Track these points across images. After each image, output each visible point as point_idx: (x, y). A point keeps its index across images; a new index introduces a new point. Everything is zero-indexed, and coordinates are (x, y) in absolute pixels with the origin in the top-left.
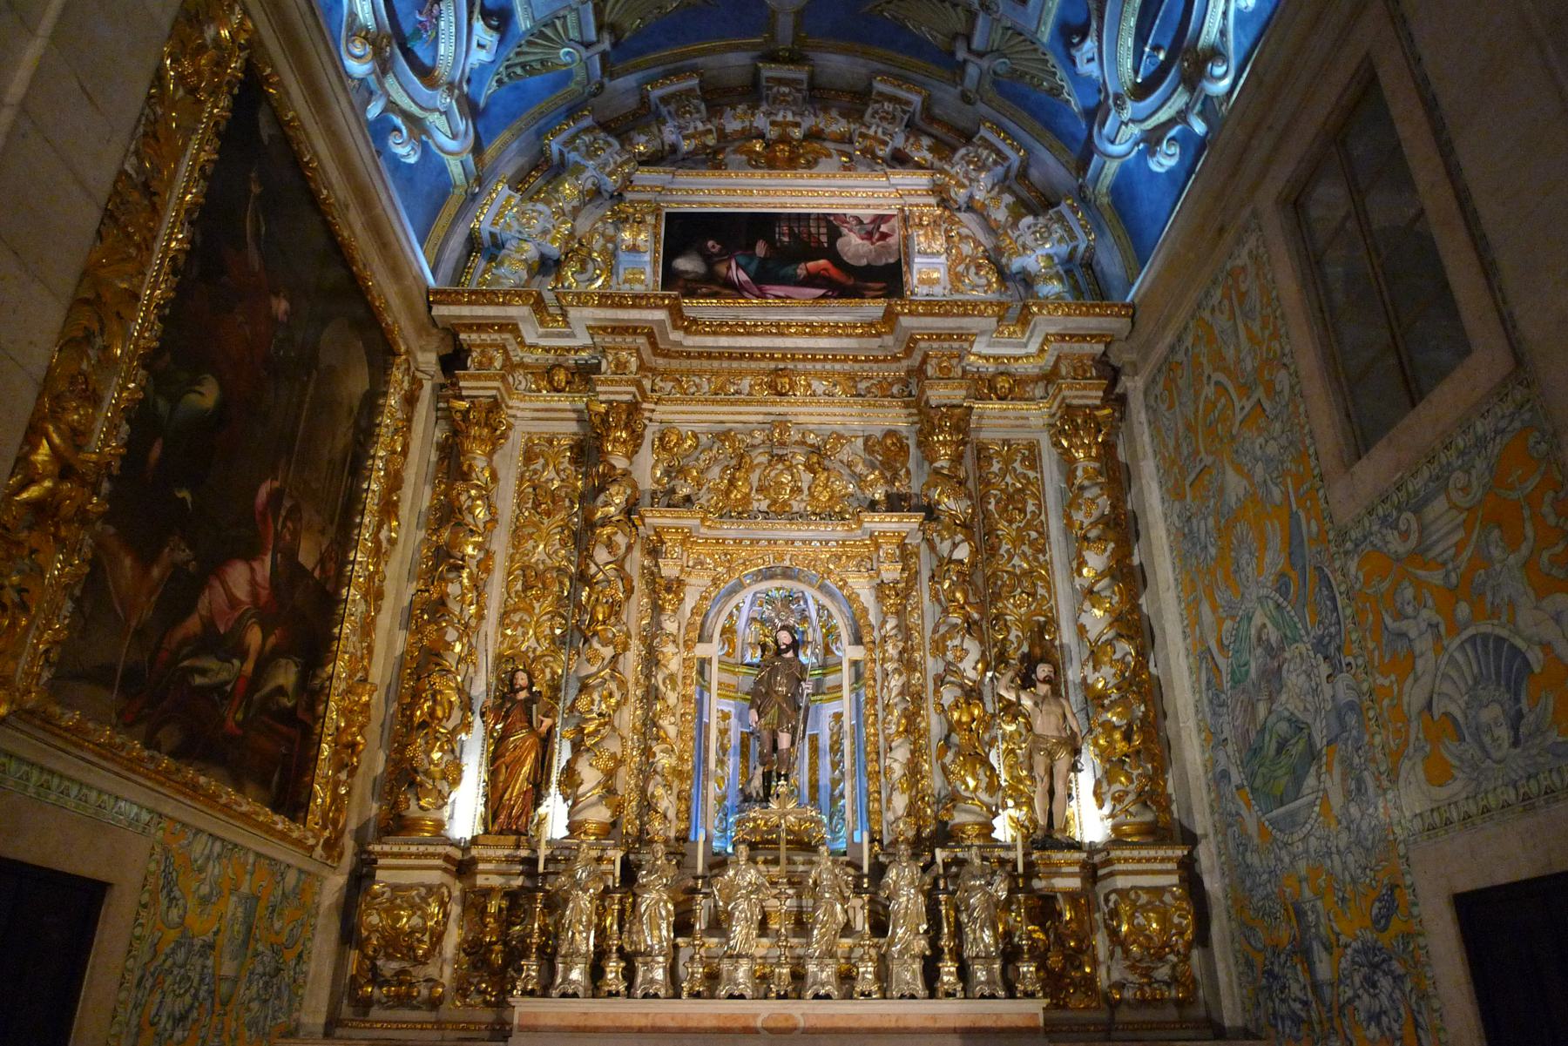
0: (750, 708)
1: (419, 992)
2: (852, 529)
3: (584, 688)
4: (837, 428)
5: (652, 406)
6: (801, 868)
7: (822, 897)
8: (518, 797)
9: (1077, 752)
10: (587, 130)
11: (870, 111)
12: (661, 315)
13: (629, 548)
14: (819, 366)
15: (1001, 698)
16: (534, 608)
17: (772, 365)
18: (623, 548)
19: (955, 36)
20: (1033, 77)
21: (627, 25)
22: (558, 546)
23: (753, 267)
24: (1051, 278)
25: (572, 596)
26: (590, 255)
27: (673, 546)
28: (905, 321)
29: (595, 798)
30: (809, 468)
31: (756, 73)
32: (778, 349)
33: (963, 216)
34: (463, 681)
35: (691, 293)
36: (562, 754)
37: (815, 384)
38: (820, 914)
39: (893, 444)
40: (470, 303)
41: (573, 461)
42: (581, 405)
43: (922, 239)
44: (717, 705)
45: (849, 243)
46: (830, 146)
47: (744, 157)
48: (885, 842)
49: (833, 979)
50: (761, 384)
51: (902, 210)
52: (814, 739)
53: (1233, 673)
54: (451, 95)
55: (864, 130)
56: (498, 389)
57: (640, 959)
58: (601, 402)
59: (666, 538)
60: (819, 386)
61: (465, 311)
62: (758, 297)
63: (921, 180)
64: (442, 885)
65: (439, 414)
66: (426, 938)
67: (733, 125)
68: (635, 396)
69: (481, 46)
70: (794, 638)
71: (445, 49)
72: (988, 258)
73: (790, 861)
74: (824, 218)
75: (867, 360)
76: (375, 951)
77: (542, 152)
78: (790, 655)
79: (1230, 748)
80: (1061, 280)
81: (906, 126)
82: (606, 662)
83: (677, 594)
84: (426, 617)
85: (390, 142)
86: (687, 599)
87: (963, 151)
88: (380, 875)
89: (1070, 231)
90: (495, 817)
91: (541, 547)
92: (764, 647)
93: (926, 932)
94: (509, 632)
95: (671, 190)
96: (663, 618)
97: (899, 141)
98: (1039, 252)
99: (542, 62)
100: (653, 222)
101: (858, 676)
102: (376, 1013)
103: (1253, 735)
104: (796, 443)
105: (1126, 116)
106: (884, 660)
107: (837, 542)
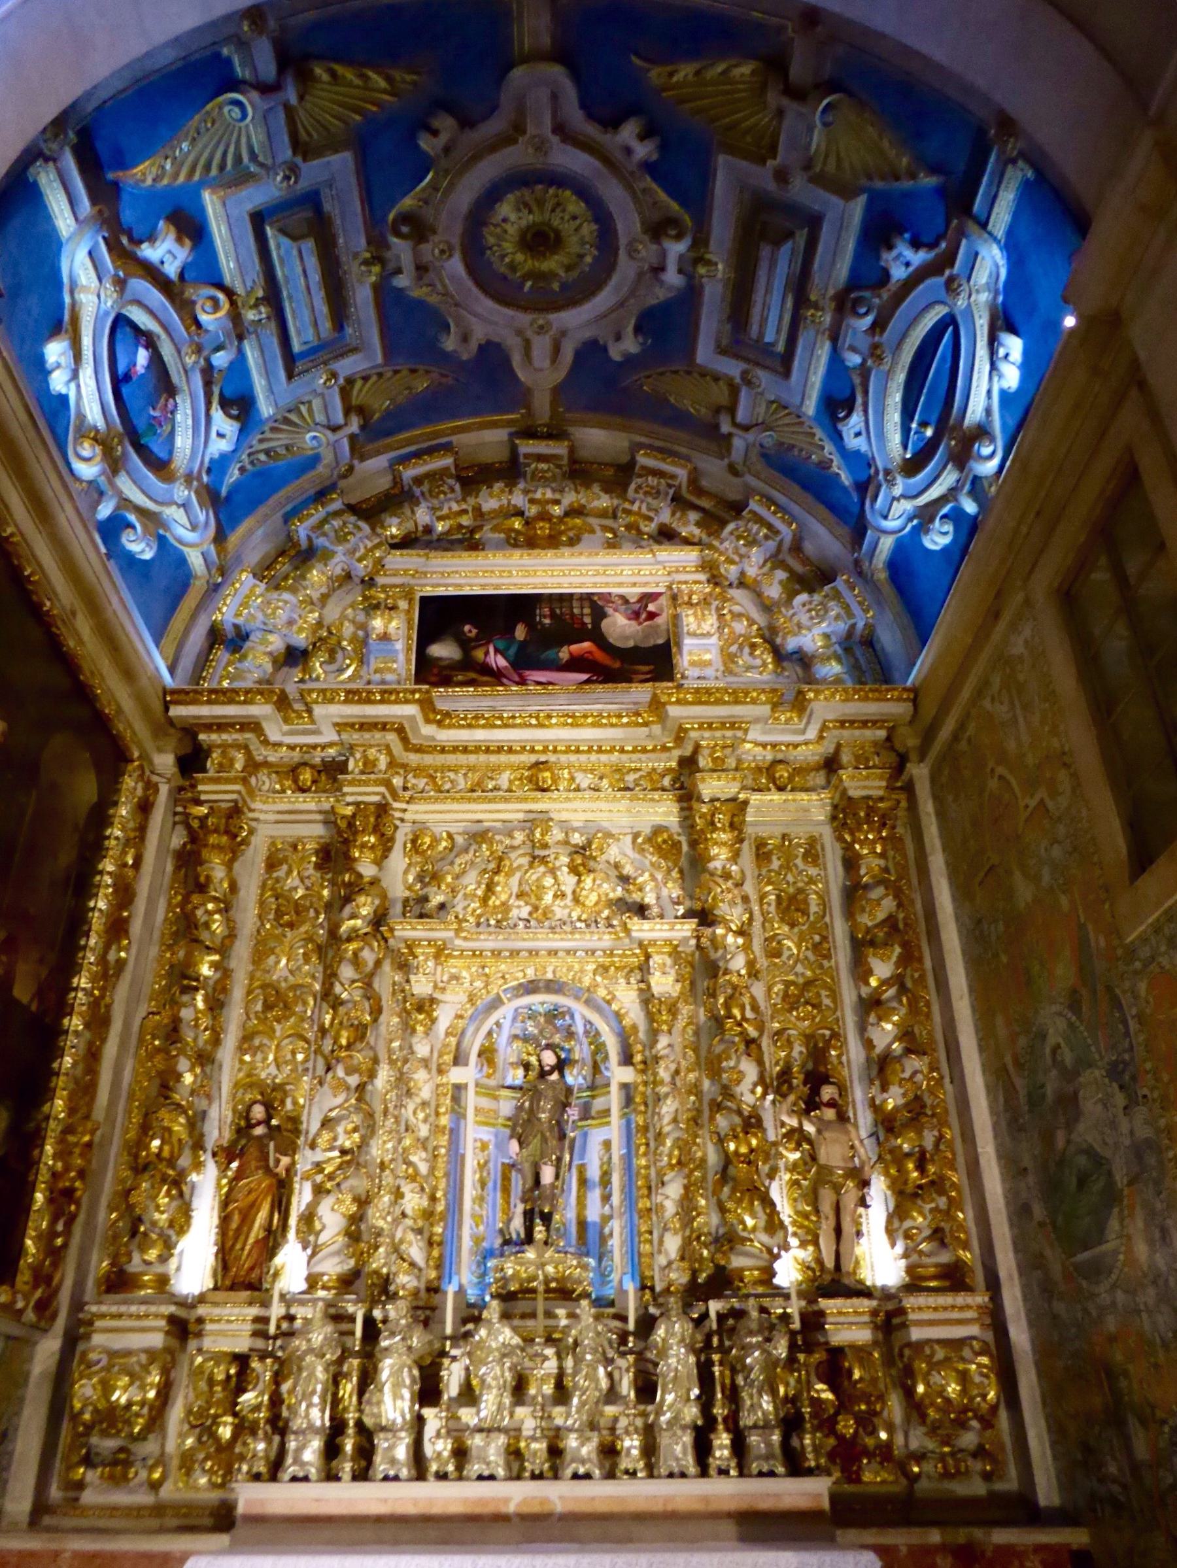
0: (511, 1137)
2: (619, 938)
5: (404, 806)
6: (564, 1322)
7: (583, 1359)
9: (866, 1183)
10: (337, 514)
11: (633, 486)
12: (411, 710)
15: (783, 1124)
16: (274, 1031)
18: (371, 964)
19: (718, 410)
21: (376, 406)
22: (301, 961)
23: (512, 651)
24: (829, 659)
25: (316, 1017)
26: (339, 643)
27: (426, 960)
30: (574, 870)
33: (735, 593)
36: (302, 1197)
38: (580, 1380)
40: (209, 702)
41: (318, 867)
43: (691, 619)
44: (474, 1133)
45: (615, 624)
46: (594, 522)
48: (658, 1289)
49: (594, 1456)
52: (582, 1170)
53: (1029, 1095)
55: (627, 505)
56: (239, 792)
57: (382, 1435)
58: (348, 804)
60: (584, 780)
61: (204, 711)
62: (518, 684)
63: (690, 556)
66: (145, 1411)
69: (220, 435)
70: (558, 1057)
71: (183, 442)
72: (762, 637)
73: (549, 1314)
74: (587, 598)
75: (634, 751)
77: (289, 538)
78: (555, 1077)
80: (839, 659)
81: (673, 500)
85: (124, 540)
87: (731, 526)
88: (97, 1339)
89: (847, 608)
93: (698, 1398)
94: (247, 1058)
95: (425, 573)
96: (415, 1040)
97: (665, 516)
98: (817, 631)
99: (287, 447)
101: (628, 1101)
104: (558, 843)
105: (897, 491)
106: (655, 1083)
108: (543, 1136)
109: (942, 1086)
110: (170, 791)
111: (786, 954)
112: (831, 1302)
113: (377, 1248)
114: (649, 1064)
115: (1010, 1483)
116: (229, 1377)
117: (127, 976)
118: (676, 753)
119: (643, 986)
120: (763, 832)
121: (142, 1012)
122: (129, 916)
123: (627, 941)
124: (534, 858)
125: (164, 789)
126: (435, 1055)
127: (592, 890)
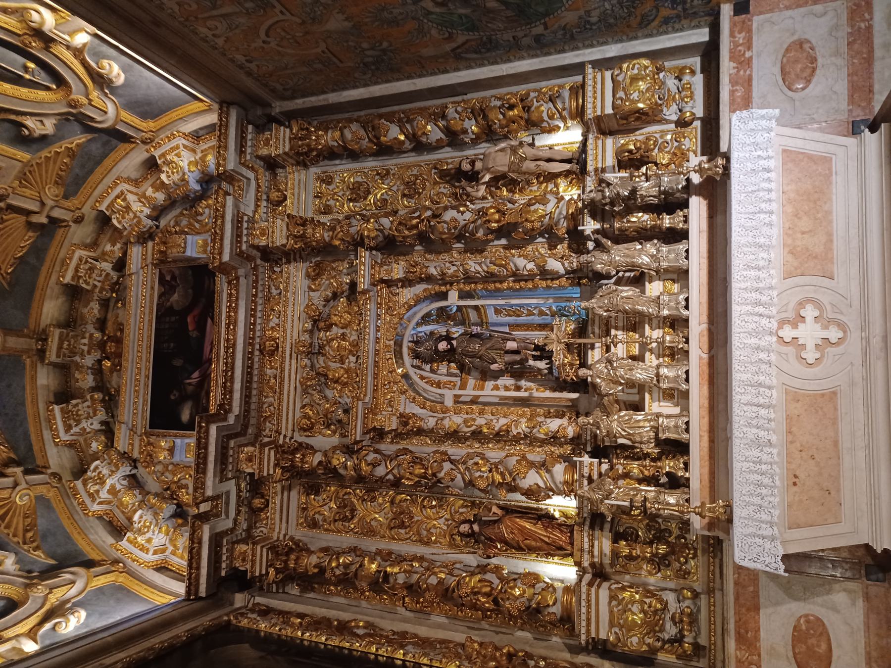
1: (688, 607)
3: (470, 484)
4: (302, 309)
5: (282, 437)
8: (547, 531)
11: (84, 286)
12: (213, 429)
13: (377, 451)
14: (259, 321)
16: (418, 521)
18: (376, 455)
20: (61, 170)
27: (377, 420)
28: (226, 257)
29: (547, 475)
30: (329, 328)
31: (51, 364)
34: (466, 572)
36: (518, 499)
37: (272, 324)
42: (279, 487)
45: (177, 301)
47: (115, 374)
53: (467, 29)
54: (35, 585)
55: (97, 290)
56: (262, 547)
58: (275, 472)
59: (370, 426)
61: (204, 571)
62: (211, 364)
64: (609, 588)
65: (281, 591)
66: (648, 601)
67: (89, 381)
68: (272, 448)
76: (658, 640)
78: (454, 342)
79: (520, 34)
81: (97, 261)
82: (454, 467)
84: (421, 600)
85: (64, 632)
88: (603, 636)
90: (561, 548)
93: (641, 244)
95: (133, 426)
96: (425, 427)
99: (26, 517)
102: (703, 641)
103: (509, 13)
107: (378, 308)
109: (469, 100)
110: (260, 596)
111: (385, 197)
112: (589, 163)
114: (445, 280)
117: (377, 621)
118: (259, 262)
119: (400, 285)
121: (402, 610)
122: (337, 620)
123: (372, 294)
124: (319, 353)
125: (258, 600)
127: (341, 317)
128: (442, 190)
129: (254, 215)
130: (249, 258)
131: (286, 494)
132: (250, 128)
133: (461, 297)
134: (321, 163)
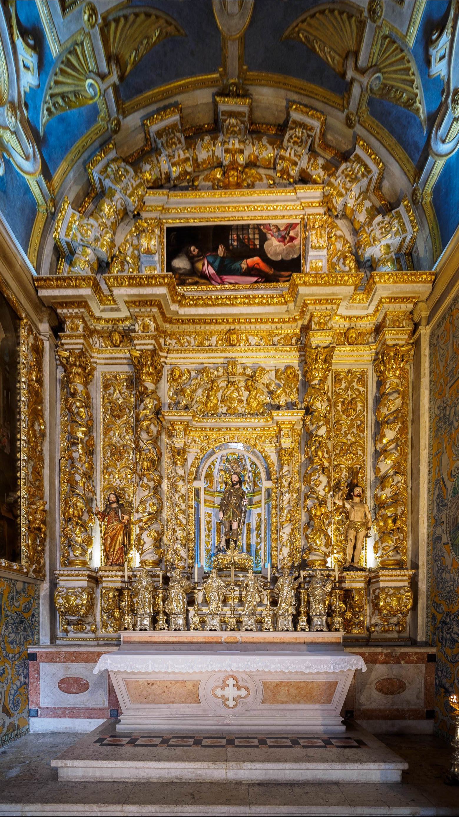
5: (165, 354)
10: (114, 160)
11: (287, 136)
14: (253, 326)
17: (228, 327)
23: (217, 263)
25: (134, 459)
26: (125, 259)
30: (247, 389)
31: (215, 104)
32: (230, 315)
35: (182, 283)
37: (251, 338)
39: (291, 373)
41: (128, 387)
46: (262, 171)
47: (210, 184)
48: (279, 568)
50: (222, 340)
51: (303, 219)
60: (253, 340)
62: (219, 284)
67: (203, 155)
83: (183, 457)
86: (189, 459)
87: (343, 166)
89: (402, 225)
91: (117, 434)
92: (226, 484)
95: (168, 209)
97: (304, 163)
100: (159, 233)
101: (269, 496)
107: (260, 428)
108: (233, 510)
110: (50, 345)
113: (168, 552)
115: (406, 635)
116: (114, 596)
117: (47, 439)
118: (300, 323)
119: (277, 444)
120: (339, 368)
125: (47, 344)
126: (187, 475)
128: (344, 473)
129: (338, 315)
130: (303, 312)
131: (125, 361)
132: (410, 306)
133: (268, 490)
134: (375, 375)
